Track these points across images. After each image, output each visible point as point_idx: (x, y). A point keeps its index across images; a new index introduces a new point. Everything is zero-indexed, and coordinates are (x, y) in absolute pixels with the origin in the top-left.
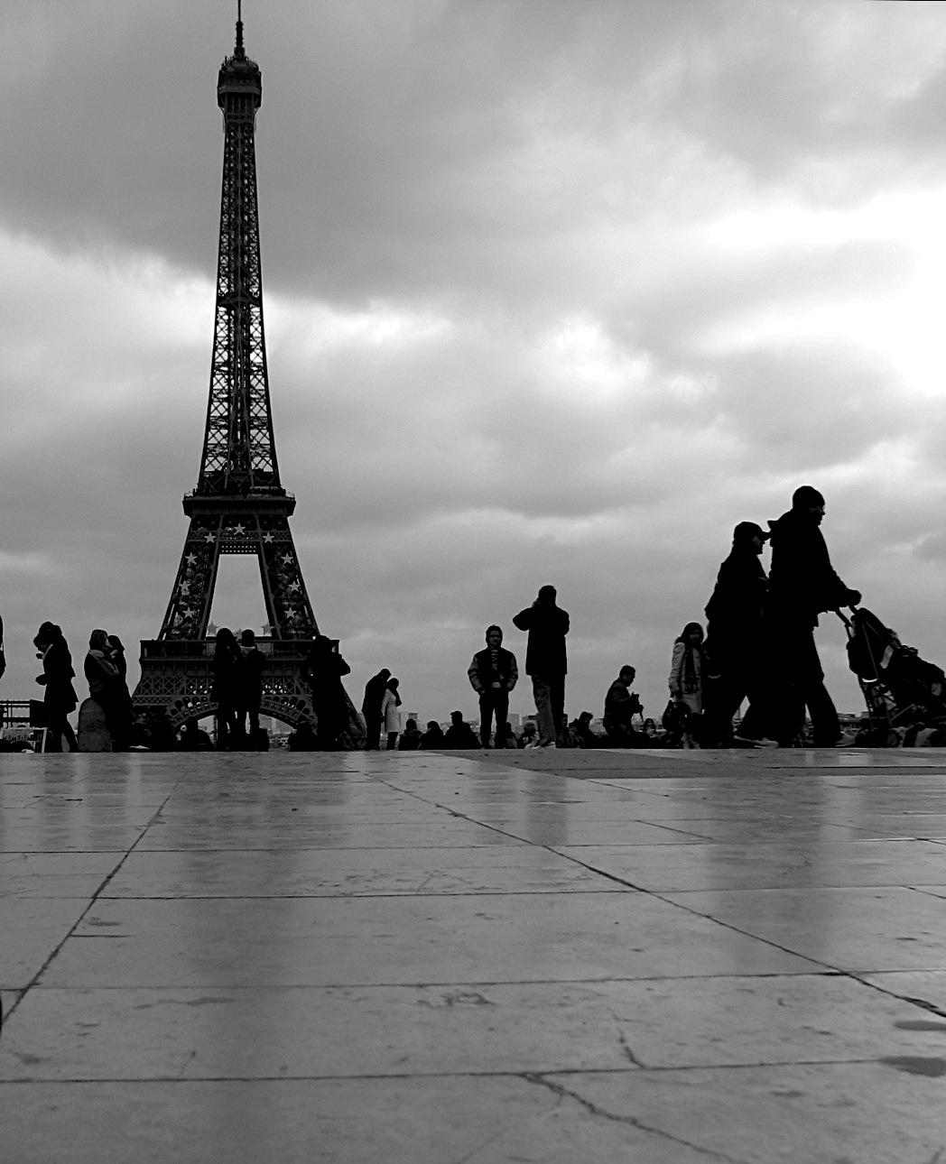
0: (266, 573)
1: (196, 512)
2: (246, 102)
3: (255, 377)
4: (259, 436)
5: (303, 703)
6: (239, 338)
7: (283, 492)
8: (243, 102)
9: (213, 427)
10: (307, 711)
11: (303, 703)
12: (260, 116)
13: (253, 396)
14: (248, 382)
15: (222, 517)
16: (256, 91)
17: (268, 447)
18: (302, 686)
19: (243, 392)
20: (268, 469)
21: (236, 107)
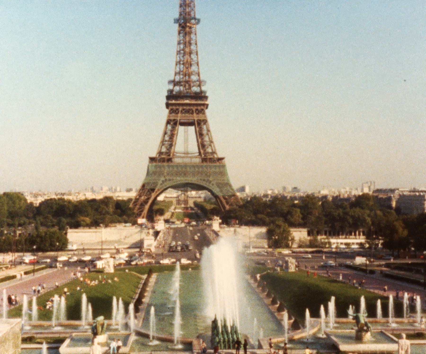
0: (198, 132)
1: (170, 107)
4: (194, 78)
6: (187, 39)
10: (213, 185)
13: (193, 63)
14: (190, 56)
19: (189, 60)
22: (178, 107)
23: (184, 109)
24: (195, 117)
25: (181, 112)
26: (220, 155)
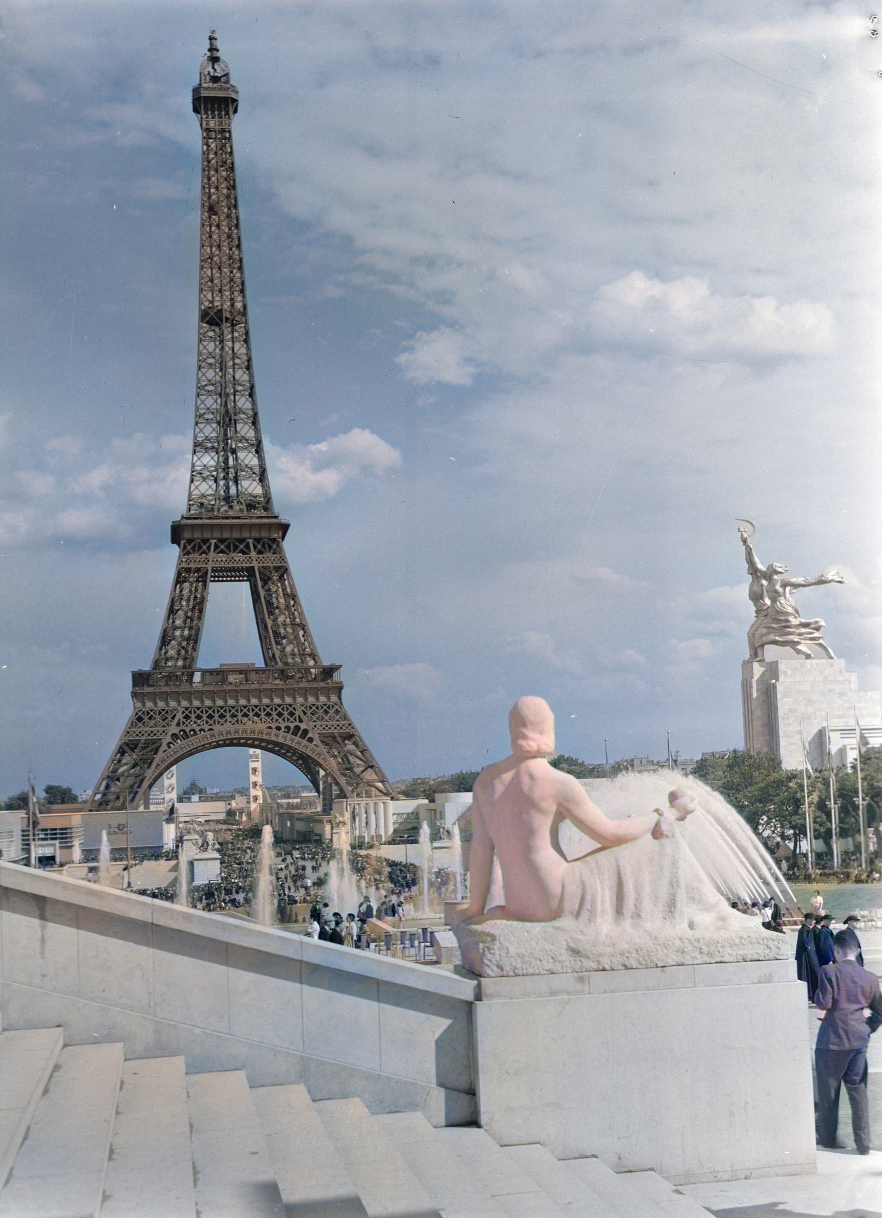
2: (223, 106)
3: (243, 395)
5: (305, 732)
7: (276, 517)
8: (219, 107)
9: (198, 449)
10: (311, 740)
11: (305, 732)
12: (238, 124)
15: (213, 542)
16: (233, 96)
17: (257, 470)
18: (305, 713)
20: (258, 490)
21: (213, 113)
22: (207, 535)
23: (222, 541)
24: (254, 559)
25: (216, 547)
26: (326, 662)
